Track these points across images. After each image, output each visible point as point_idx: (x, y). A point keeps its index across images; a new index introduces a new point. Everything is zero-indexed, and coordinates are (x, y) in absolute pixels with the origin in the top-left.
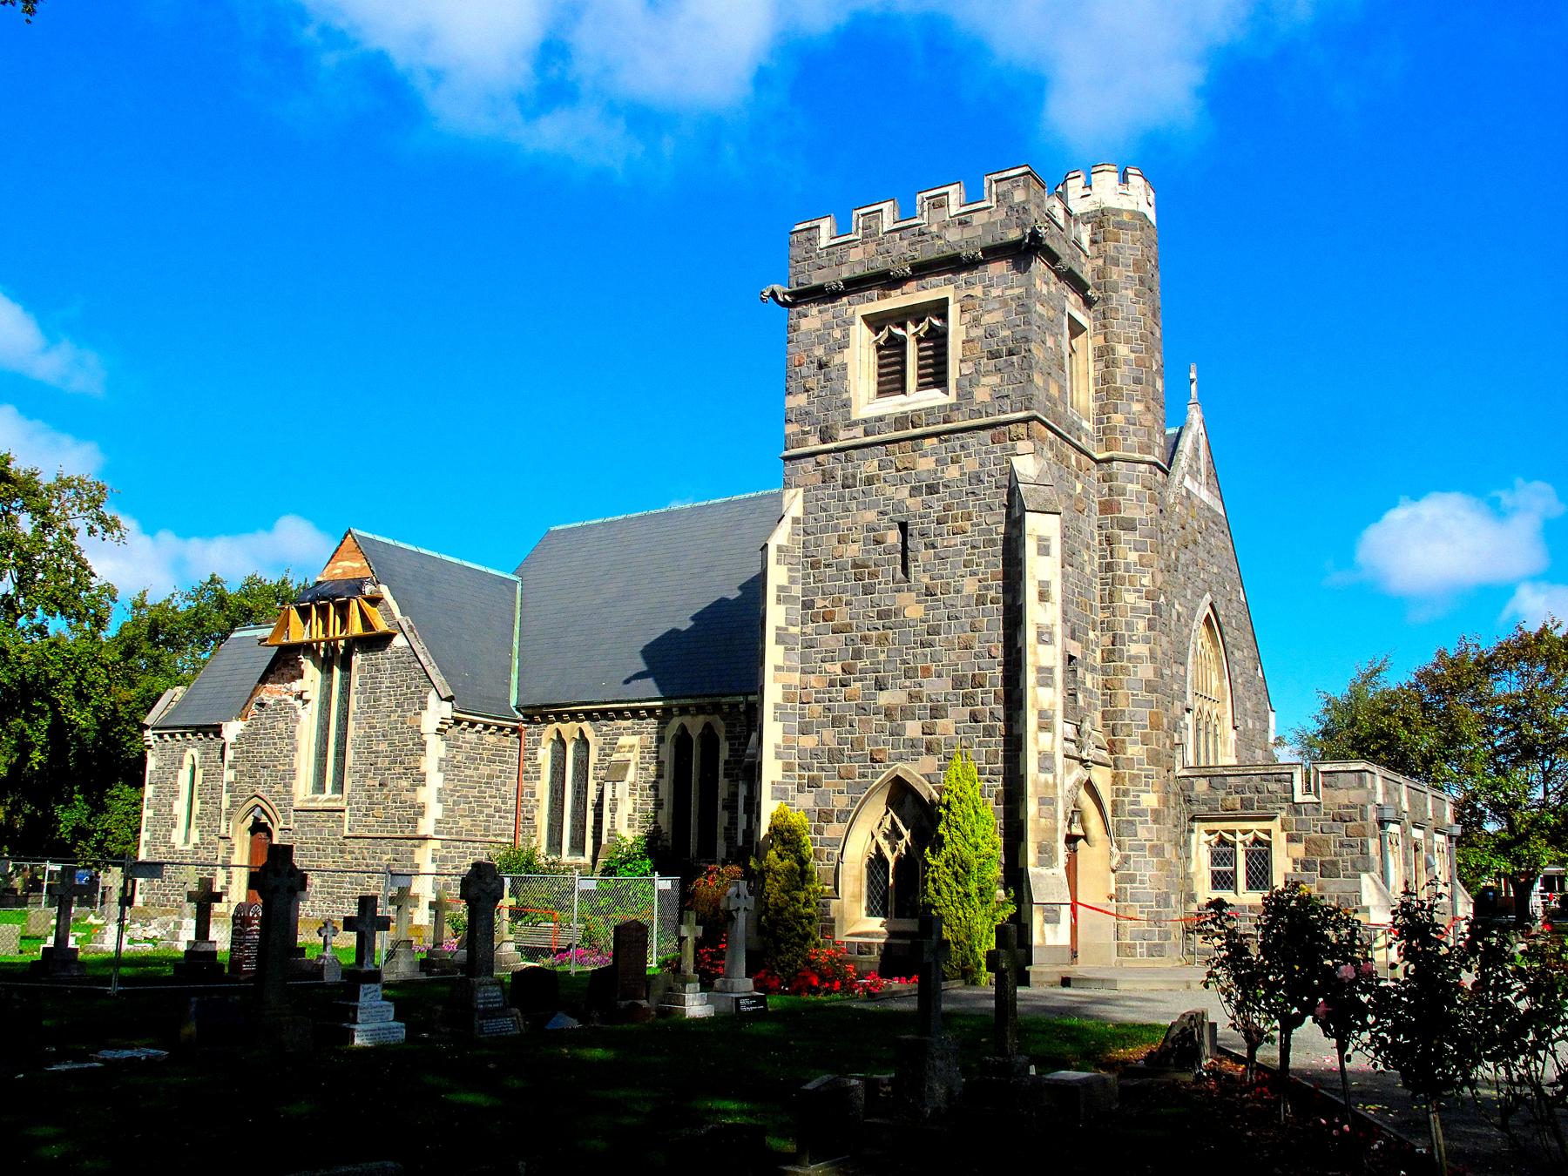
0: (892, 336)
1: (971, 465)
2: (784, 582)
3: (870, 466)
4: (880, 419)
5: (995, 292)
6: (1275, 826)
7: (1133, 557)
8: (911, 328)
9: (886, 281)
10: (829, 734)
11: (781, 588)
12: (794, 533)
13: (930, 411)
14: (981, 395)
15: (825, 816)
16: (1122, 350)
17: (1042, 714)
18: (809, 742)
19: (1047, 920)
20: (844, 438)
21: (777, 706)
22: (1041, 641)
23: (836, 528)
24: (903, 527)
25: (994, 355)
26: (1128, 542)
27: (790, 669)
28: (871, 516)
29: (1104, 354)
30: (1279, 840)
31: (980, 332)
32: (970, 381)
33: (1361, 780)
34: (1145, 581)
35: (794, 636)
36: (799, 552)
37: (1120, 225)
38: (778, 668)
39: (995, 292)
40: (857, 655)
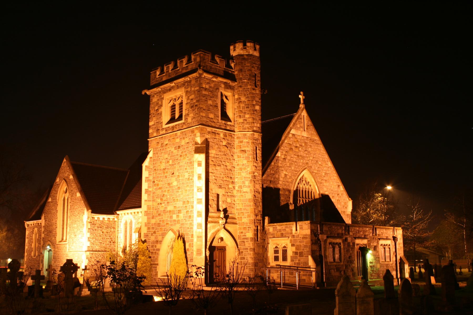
1: (187, 140)
2: (147, 176)
5: (193, 89)
11: (146, 178)
12: (150, 161)
17: (198, 212)
20: (161, 133)
27: (149, 201)
28: (166, 156)
35: (150, 191)
36: (152, 167)
38: (146, 201)
39: (193, 89)
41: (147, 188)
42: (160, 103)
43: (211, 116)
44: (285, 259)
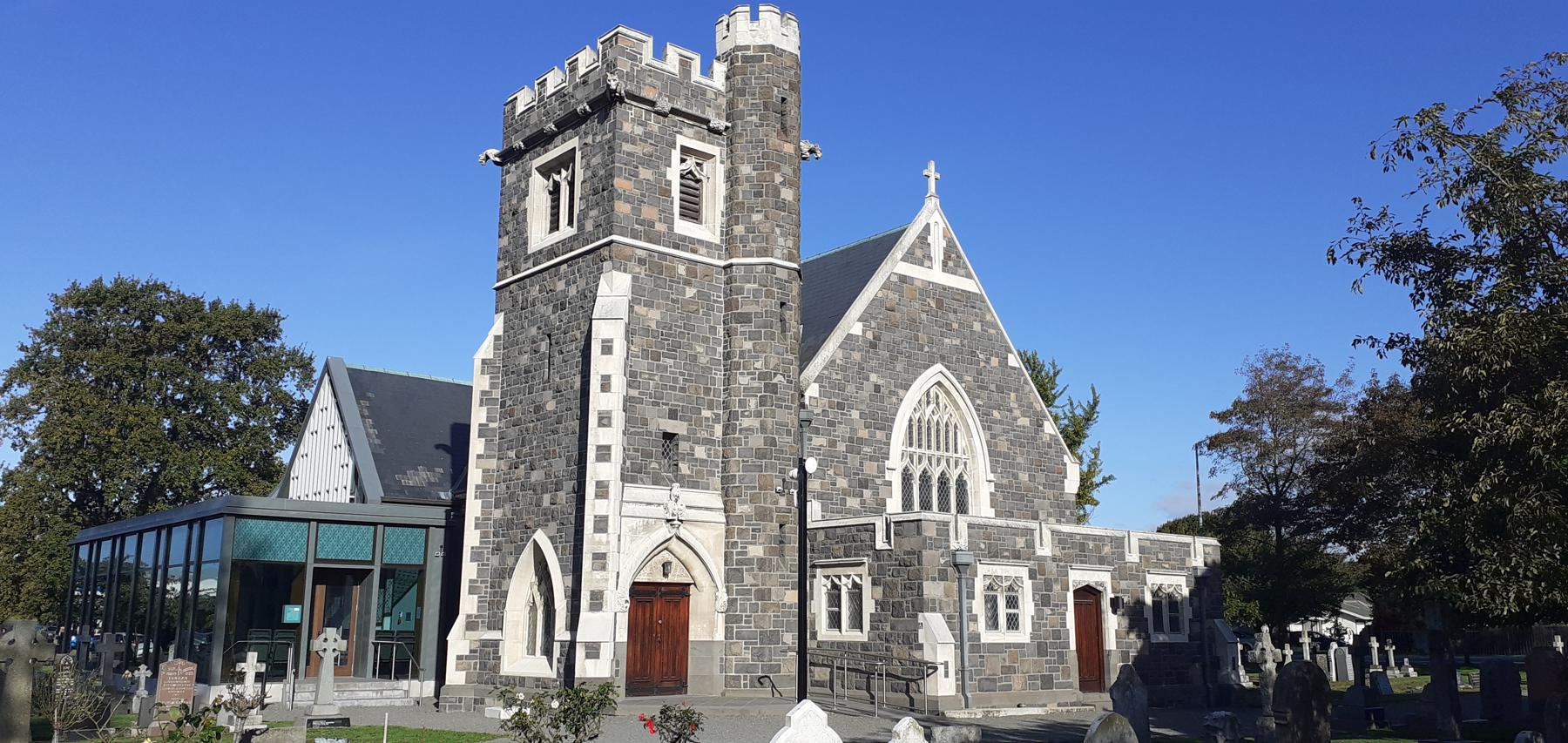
5: (598, 138)
6: (864, 570)
7: (748, 345)
12: (496, 348)
14: (589, 226)
16: (746, 169)
18: (497, 514)
19: (588, 656)
21: (477, 487)
22: (601, 424)
25: (596, 192)
26: (743, 333)
27: (489, 457)
29: (732, 177)
30: (866, 584)
31: (589, 173)
32: (584, 215)
33: (919, 528)
34: (758, 365)
37: (746, 59)
38: (479, 456)
39: (598, 138)
41: (484, 421)
43: (649, 212)
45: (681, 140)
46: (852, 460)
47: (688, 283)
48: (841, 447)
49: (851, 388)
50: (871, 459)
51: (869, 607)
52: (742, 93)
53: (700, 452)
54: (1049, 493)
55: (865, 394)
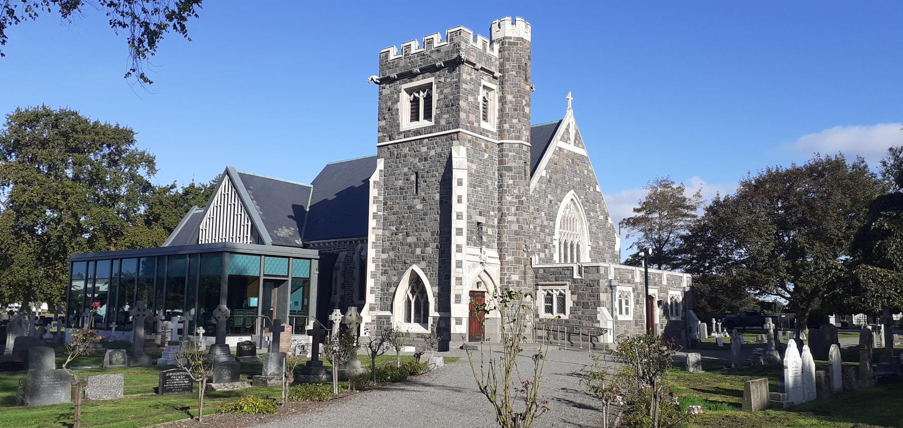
0: (415, 97)
1: (439, 150)
3: (406, 150)
4: (409, 131)
5: (448, 80)
7: (511, 182)
8: (421, 93)
9: (411, 76)
10: (391, 253)
11: (375, 197)
13: (425, 128)
14: (443, 122)
15: (389, 285)
16: (509, 97)
18: (385, 256)
19: (457, 324)
22: (458, 218)
23: (394, 174)
24: (417, 173)
25: (447, 106)
28: (406, 169)
29: (502, 100)
31: (443, 96)
37: (510, 43)
38: (374, 228)
39: (448, 80)
40: (401, 223)
42: (395, 96)
43: (472, 118)
44: (562, 309)
45: (484, 82)
46: (542, 235)
47: (485, 151)
48: (538, 229)
49: (541, 201)
50: (549, 235)
51: (569, 304)
52: (508, 60)
53: (490, 231)
54: (610, 251)
55: (546, 205)
